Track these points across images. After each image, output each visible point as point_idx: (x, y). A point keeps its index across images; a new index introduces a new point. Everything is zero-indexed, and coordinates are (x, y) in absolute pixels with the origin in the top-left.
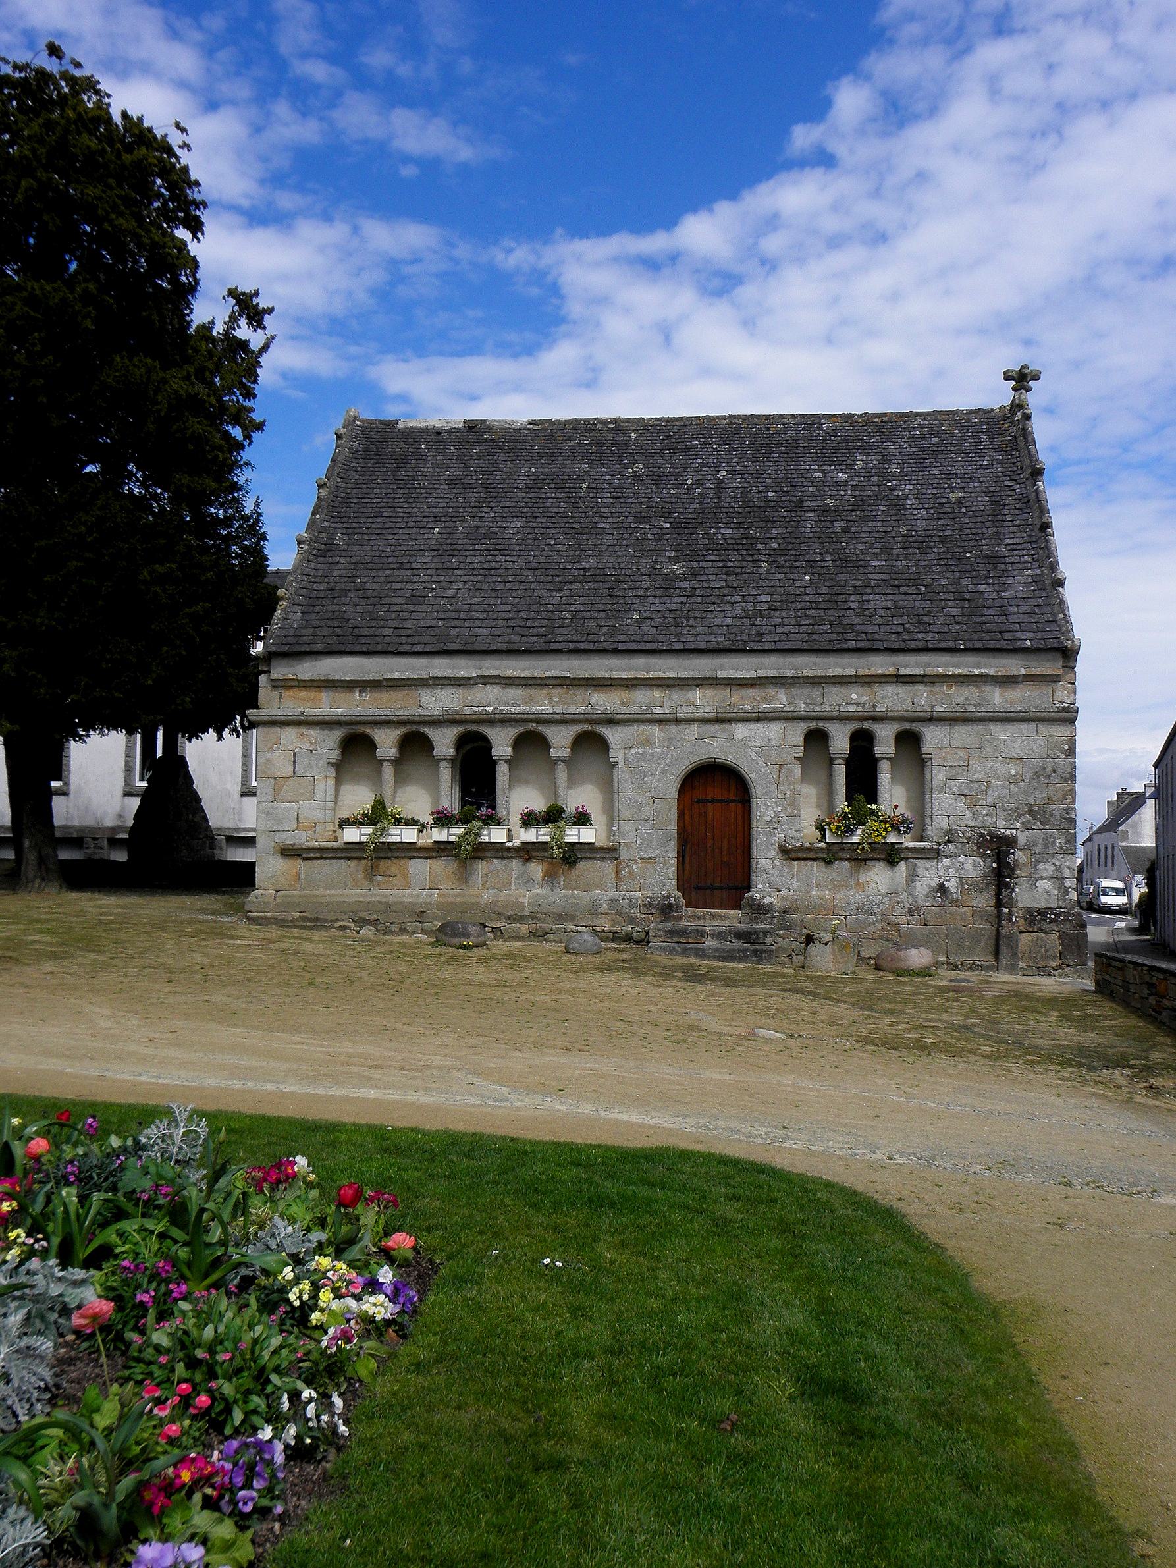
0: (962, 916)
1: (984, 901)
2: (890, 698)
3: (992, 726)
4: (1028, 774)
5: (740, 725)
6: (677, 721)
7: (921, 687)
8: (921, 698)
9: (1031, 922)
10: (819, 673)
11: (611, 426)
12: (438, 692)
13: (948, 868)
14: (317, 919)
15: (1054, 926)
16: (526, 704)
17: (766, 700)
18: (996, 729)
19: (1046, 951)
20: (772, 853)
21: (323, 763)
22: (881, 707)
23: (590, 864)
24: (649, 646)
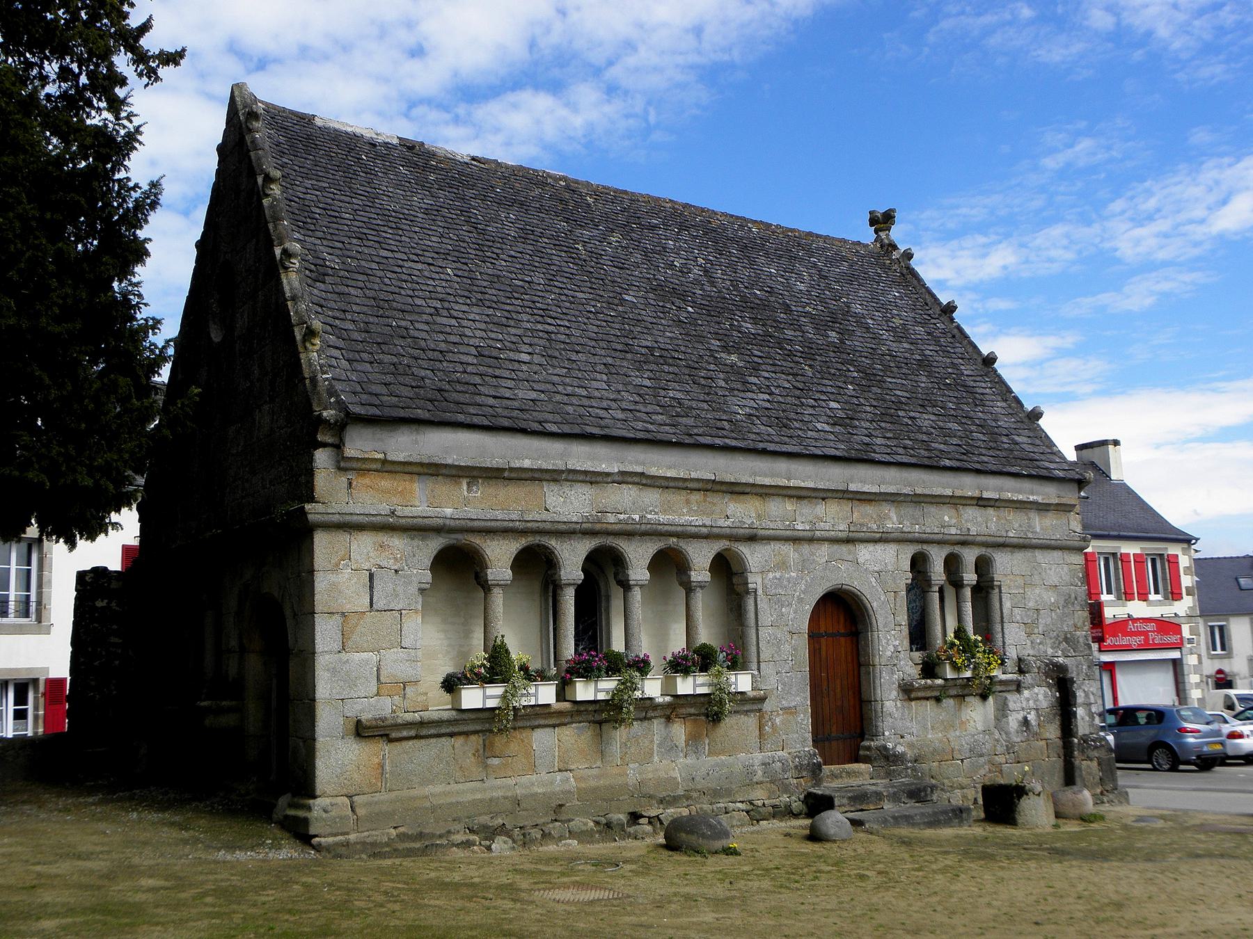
14: (421, 836)
16: (665, 512)
18: (1040, 555)
20: (895, 693)
21: (413, 589)
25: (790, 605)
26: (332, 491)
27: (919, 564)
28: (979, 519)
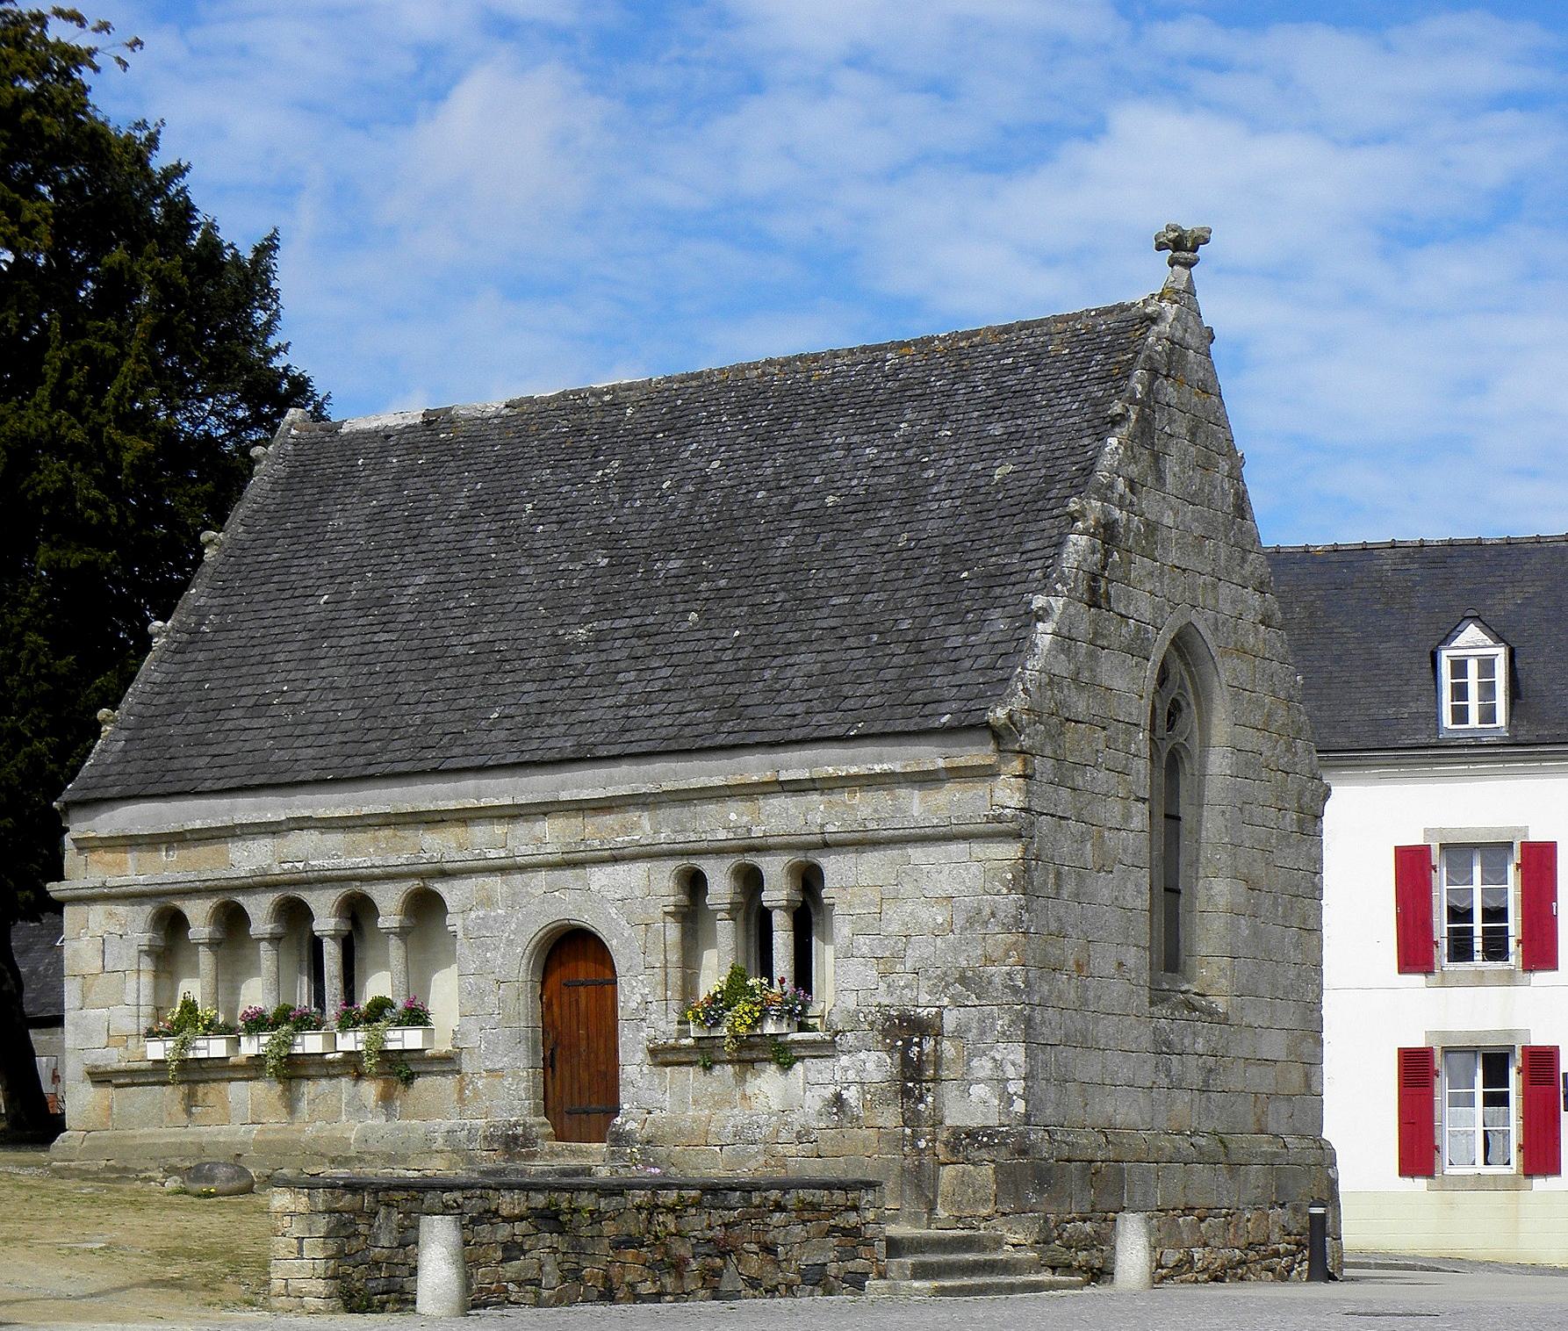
0: (867, 1138)
1: (890, 1117)
2: (780, 817)
4: (960, 921)
6: (522, 869)
7: (815, 797)
10: (682, 785)
11: (607, 398)
12: (249, 843)
14: (125, 1169)
17: (626, 830)
18: (916, 853)
21: (134, 952)
22: (757, 832)
23: (429, 1080)
24: (478, 761)
25: (497, 948)
26: (81, 871)
27: (694, 883)
28: (793, 811)
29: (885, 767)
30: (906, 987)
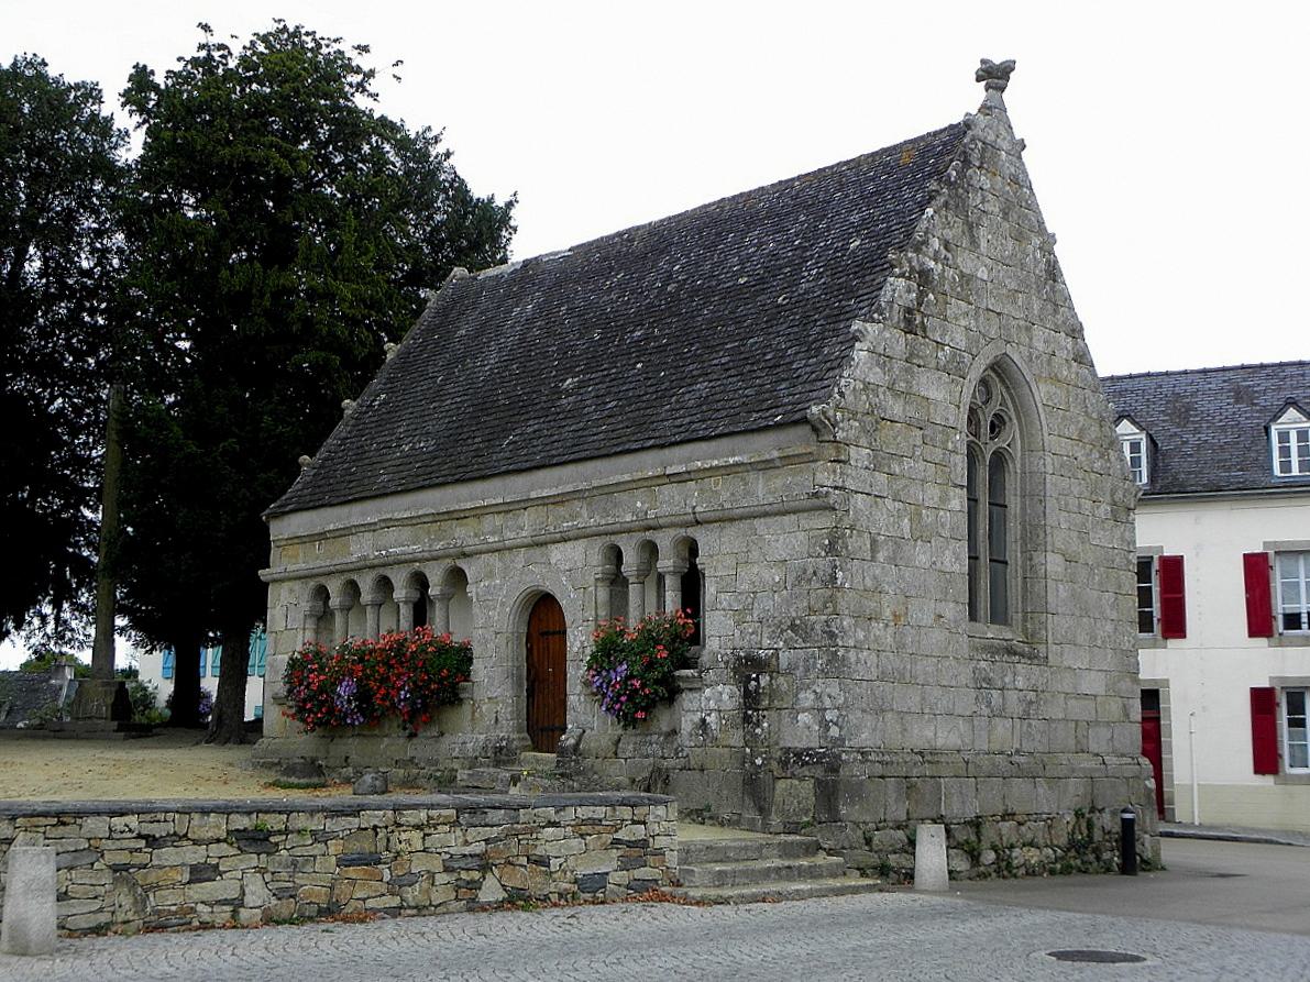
0: (722, 755)
1: (736, 738)
2: (671, 502)
3: (756, 522)
5: (553, 546)
8: (691, 499)
9: (784, 764)
13: (708, 699)
15: (806, 771)
19: (799, 803)
25: (495, 609)
26: (282, 563)
29: (736, 459)
30: (753, 633)
